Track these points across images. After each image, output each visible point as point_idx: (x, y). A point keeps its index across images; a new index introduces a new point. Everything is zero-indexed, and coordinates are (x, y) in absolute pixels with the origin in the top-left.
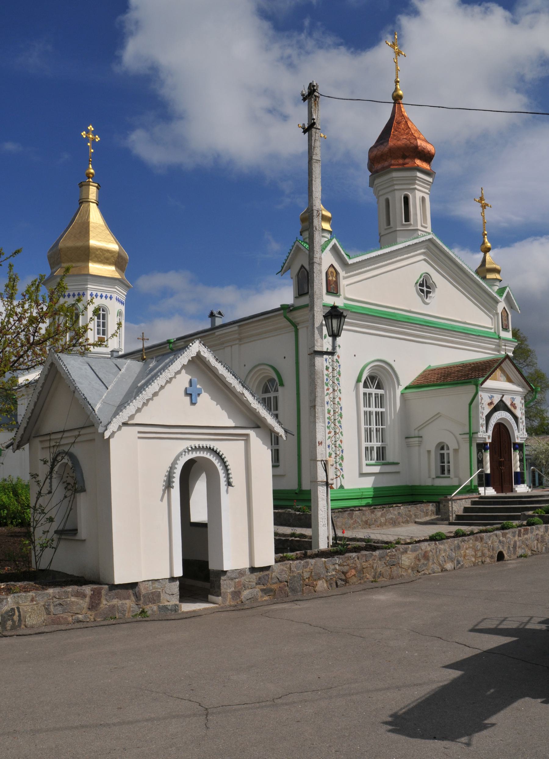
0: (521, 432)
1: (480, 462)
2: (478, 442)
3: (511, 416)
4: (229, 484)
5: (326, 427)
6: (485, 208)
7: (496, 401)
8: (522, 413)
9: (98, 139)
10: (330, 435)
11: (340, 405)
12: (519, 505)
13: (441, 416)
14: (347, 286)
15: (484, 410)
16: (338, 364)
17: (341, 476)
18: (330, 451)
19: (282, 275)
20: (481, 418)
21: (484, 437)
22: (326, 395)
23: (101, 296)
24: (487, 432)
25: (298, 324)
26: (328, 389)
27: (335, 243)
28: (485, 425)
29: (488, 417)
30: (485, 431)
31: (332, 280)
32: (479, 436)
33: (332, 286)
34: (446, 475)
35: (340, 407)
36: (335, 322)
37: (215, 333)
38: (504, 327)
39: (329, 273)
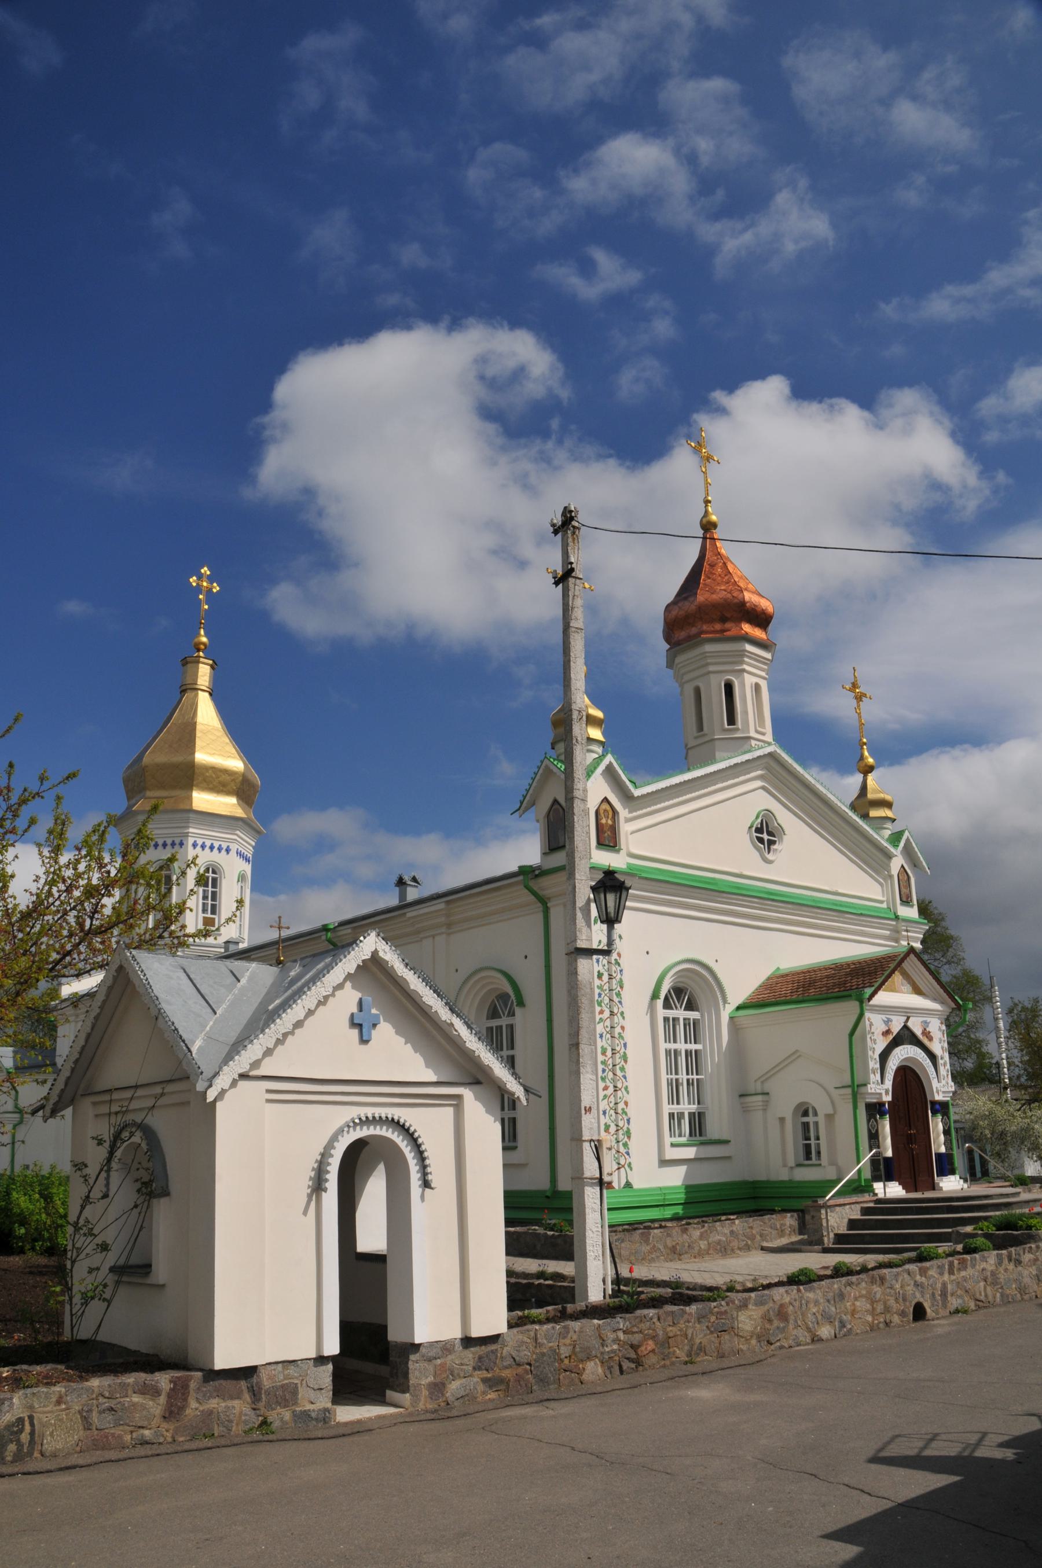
0: (944, 1082)
1: (874, 1137)
2: (868, 1100)
3: (923, 1054)
4: (426, 1184)
5: (600, 1079)
6: (861, 700)
7: (896, 1027)
8: (942, 1048)
9: (216, 589)
10: (605, 1092)
11: (623, 1038)
12: (948, 1213)
13: (799, 1056)
14: (631, 834)
15: (875, 1044)
16: (619, 969)
17: (626, 1166)
18: (606, 1121)
19: (520, 816)
20: (872, 1058)
21: (878, 1091)
22: (599, 1023)
23: (212, 848)
24: (882, 1082)
25: (549, 899)
26: (602, 1012)
27: (610, 762)
29: (884, 1057)
30: (880, 1081)
31: (607, 823)
32: (870, 1091)
33: (606, 834)
34: (814, 1161)
35: (622, 1042)
36: (611, 898)
37: (405, 913)
38: (904, 899)
39: (601, 812)
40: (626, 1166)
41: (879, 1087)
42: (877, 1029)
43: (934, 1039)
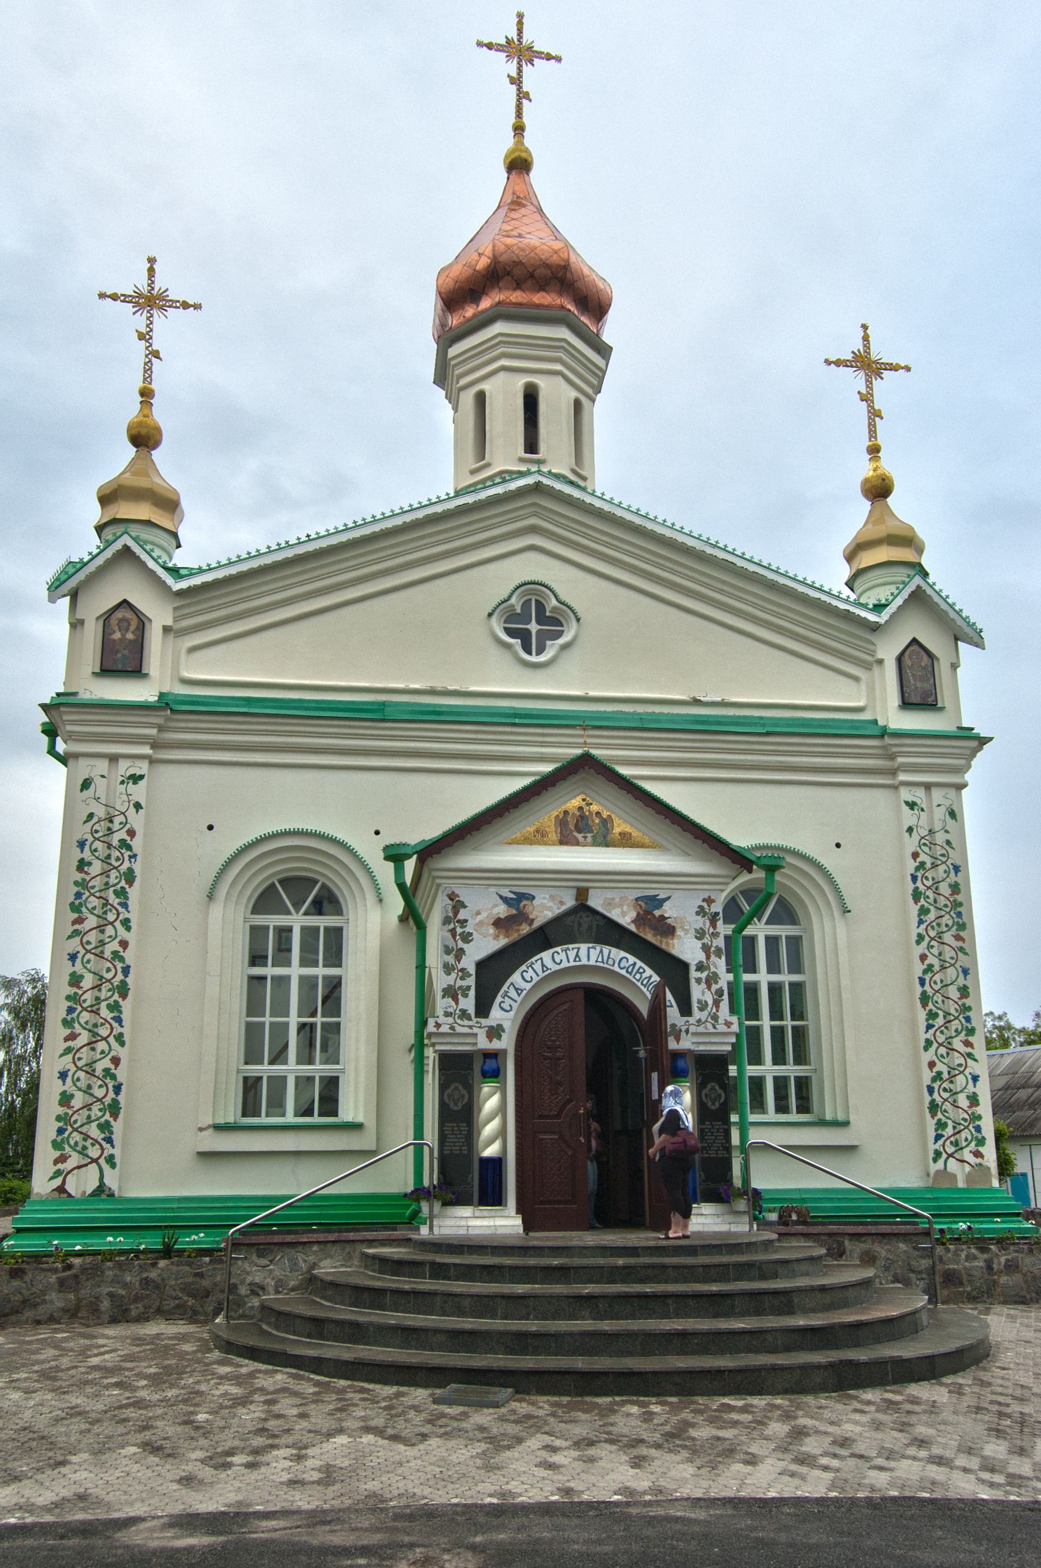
10: (70, 1043)
16: (127, 854)
18: (65, 1088)
28: (472, 993)
30: (472, 1011)
31: (123, 639)
33: (119, 655)
35: (119, 965)
40: (102, 1161)
41: (466, 1022)
42: (478, 913)
43: (679, 932)
